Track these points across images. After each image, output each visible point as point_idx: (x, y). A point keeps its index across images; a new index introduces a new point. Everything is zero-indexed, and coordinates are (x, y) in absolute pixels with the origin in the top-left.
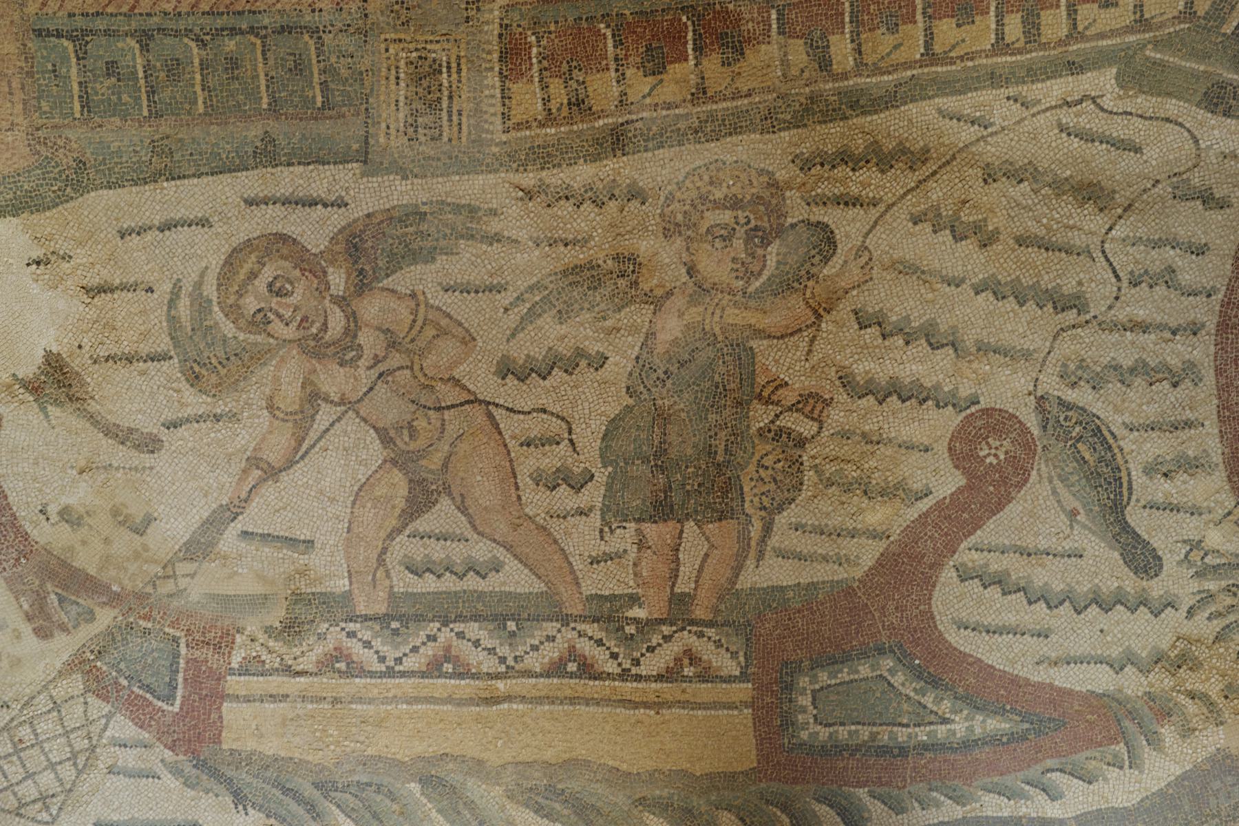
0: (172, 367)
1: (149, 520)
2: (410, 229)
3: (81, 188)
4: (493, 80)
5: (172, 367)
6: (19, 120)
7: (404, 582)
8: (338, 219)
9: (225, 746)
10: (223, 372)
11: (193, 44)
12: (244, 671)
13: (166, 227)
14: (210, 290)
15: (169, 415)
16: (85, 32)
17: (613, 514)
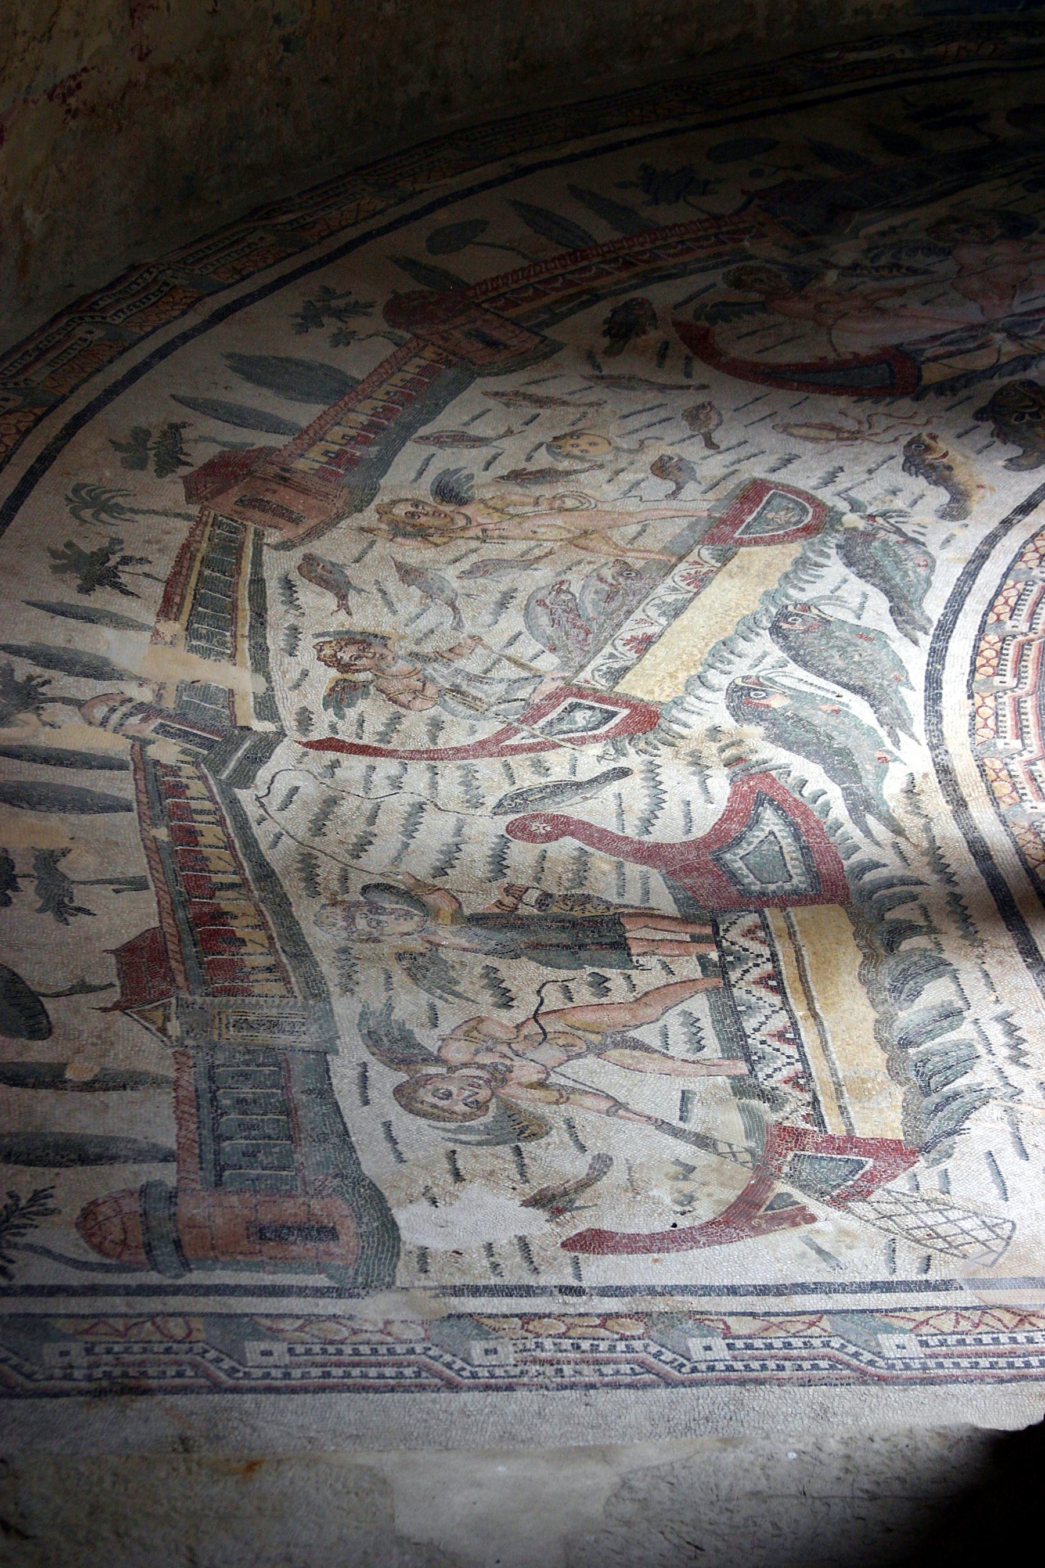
0: (528, 1148)
1: (677, 1162)
2: (385, 1039)
3: (360, 1180)
4: (254, 1000)
5: (528, 1148)
6: (301, 1200)
7: (712, 1047)
8: (377, 1069)
9: (902, 1138)
10: (525, 1123)
11: (225, 1118)
12: (821, 1123)
13: (393, 1141)
14: (452, 1126)
15: (574, 1150)
16: (216, 1162)
17: (627, 961)
